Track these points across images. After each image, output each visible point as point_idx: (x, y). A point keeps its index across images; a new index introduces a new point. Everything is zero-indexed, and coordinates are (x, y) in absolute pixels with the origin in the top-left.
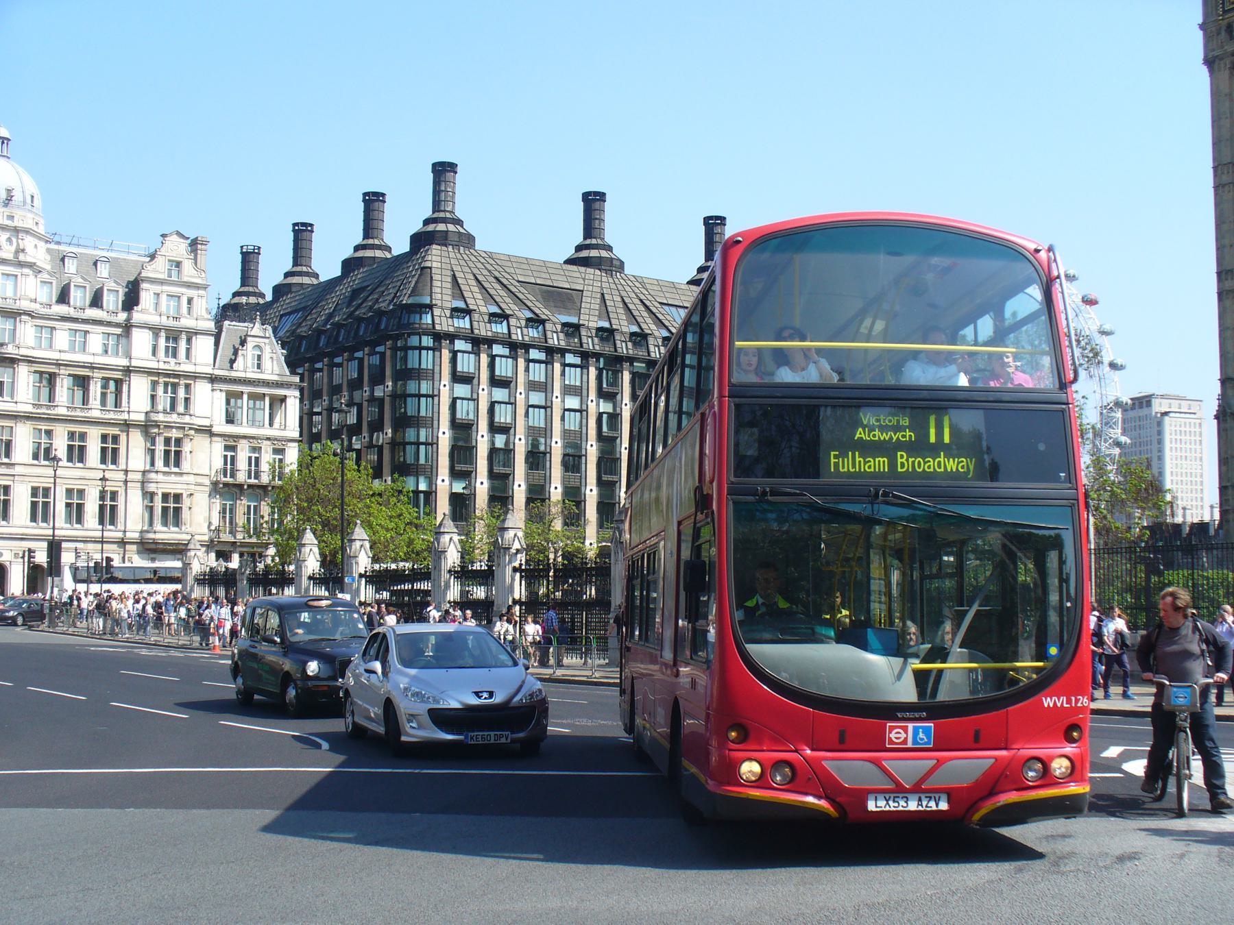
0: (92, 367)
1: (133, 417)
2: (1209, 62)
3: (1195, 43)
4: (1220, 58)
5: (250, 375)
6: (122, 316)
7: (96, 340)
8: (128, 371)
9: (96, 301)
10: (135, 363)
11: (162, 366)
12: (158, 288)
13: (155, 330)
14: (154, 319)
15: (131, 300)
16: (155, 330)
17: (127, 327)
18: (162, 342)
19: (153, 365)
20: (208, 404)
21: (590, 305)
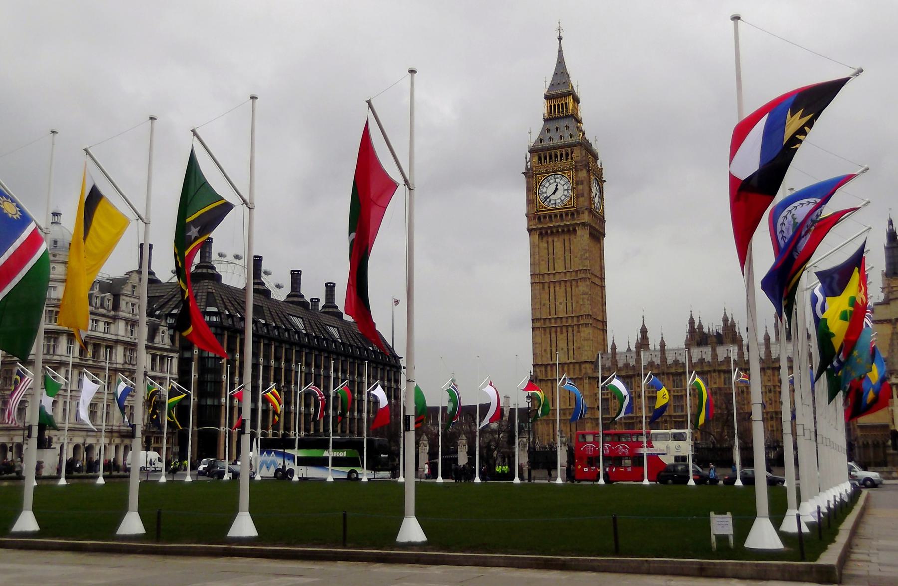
0: (103, 339)
1: (118, 366)
2: (530, 231)
3: (524, 223)
4: (535, 230)
5: (161, 346)
6: (112, 313)
7: (101, 326)
8: (117, 342)
9: (102, 306)
10: (120, 338)
11: (129, 340)
12: (128, 299)
13: (127, 321)
14: (127, 315)
15: (116, 307)
16: (127, 321)
17: (115, 318)
18: (129, 327)
19: (126, 339)
20: (144, 359)
21: (267, 313)
